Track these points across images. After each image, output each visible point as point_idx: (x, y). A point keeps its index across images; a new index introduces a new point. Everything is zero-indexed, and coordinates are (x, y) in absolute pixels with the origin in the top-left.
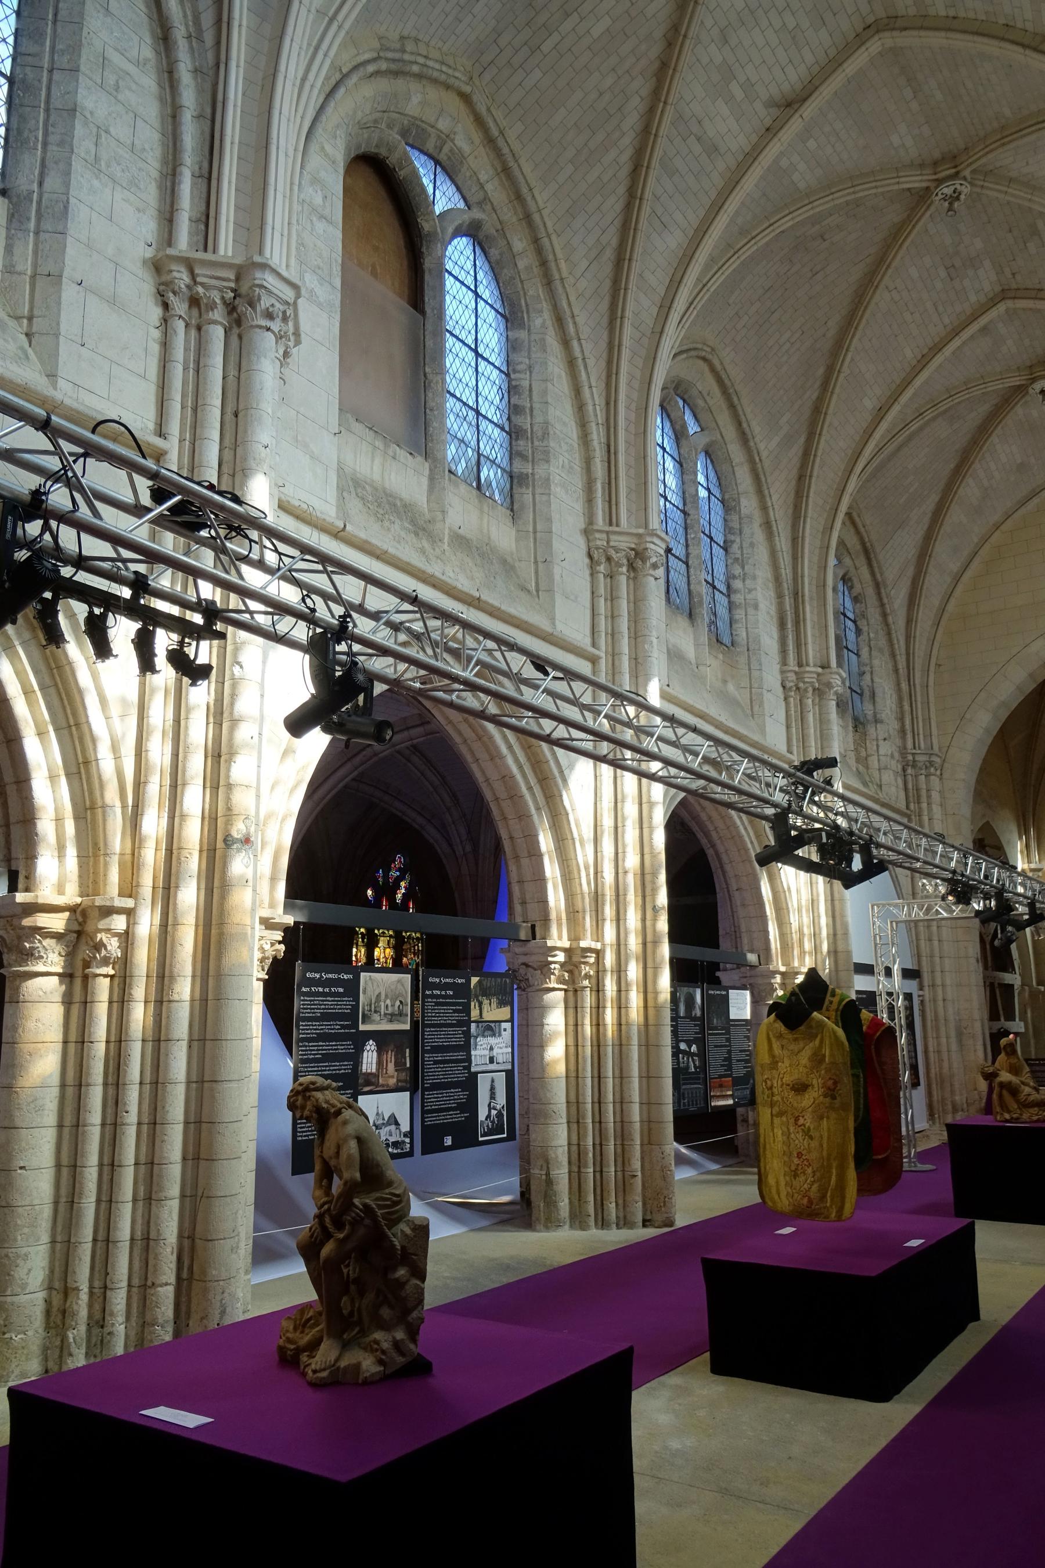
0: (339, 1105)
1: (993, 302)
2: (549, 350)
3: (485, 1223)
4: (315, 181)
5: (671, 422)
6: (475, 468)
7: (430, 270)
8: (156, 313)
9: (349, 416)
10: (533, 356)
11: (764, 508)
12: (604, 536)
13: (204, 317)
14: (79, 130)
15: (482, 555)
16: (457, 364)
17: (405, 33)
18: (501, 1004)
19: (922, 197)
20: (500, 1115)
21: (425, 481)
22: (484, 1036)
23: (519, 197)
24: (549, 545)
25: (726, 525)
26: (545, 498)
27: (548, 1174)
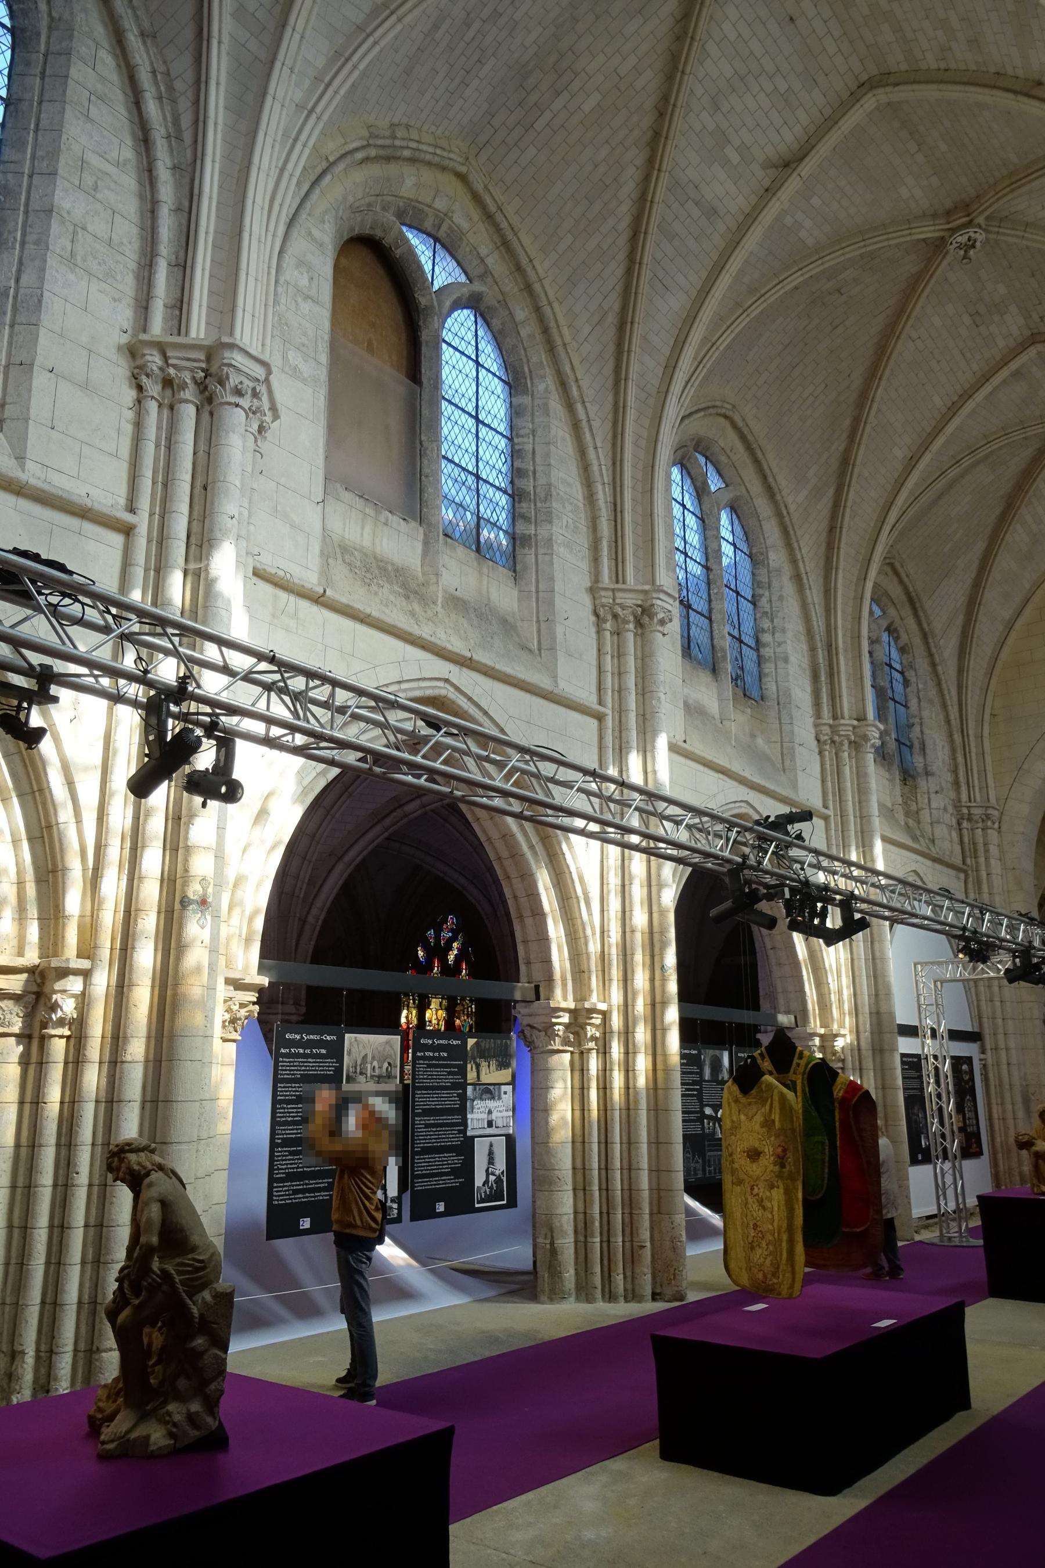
0: (150, 1167)
1: (1023, 347)
2: (551, 414)
3: (491, 1293)
4: (300, 263)
5: (692, 479)
6: (474, 532)
7: (427, 342)
8: (130, 395)
9: (338, 485)
10: (536, 420)
11: (794, 561)
12: (610, 594)
13: (177, 396)
14: (55, 227)
15: (480, 616)
16: (454, 432)
17: (396, 120)
18: (503, 1065)
19: (937, 247)
20: (499, 1180)
21: (419, 547)
22: (481, 1099)
23: (519, 268)
24: (551, 603)
25: (753, 580)
26: (547, 558)
27: (552, 1243)
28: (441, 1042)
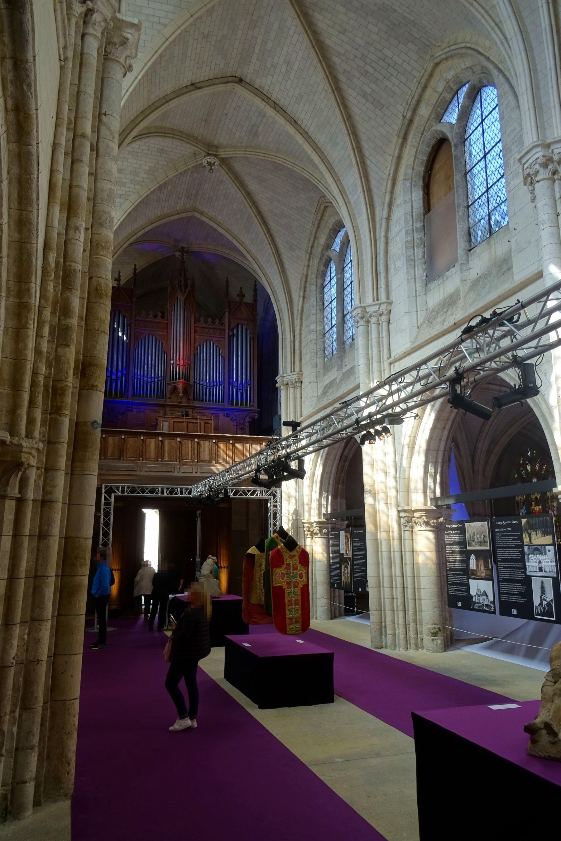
18: (545, 534)
20: (549, 604)
28: (507, 522)
